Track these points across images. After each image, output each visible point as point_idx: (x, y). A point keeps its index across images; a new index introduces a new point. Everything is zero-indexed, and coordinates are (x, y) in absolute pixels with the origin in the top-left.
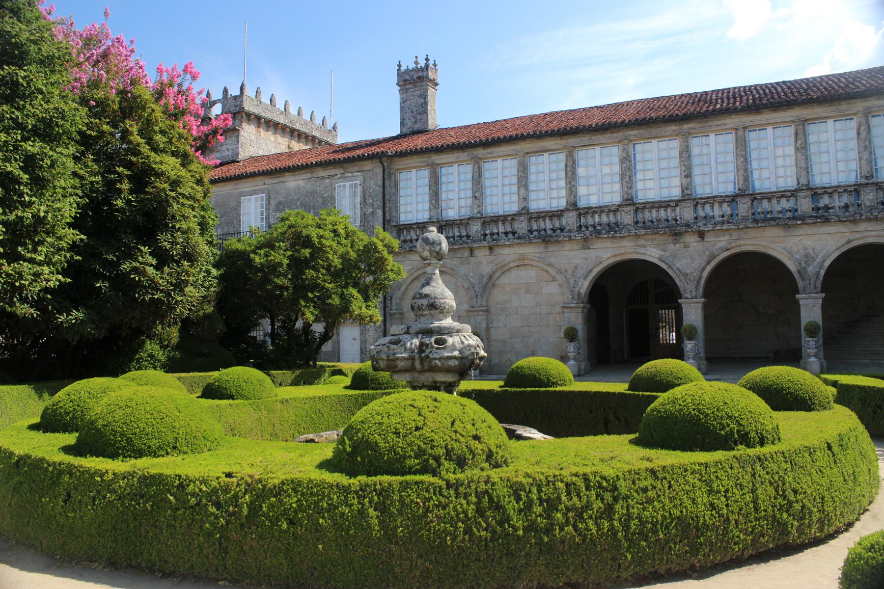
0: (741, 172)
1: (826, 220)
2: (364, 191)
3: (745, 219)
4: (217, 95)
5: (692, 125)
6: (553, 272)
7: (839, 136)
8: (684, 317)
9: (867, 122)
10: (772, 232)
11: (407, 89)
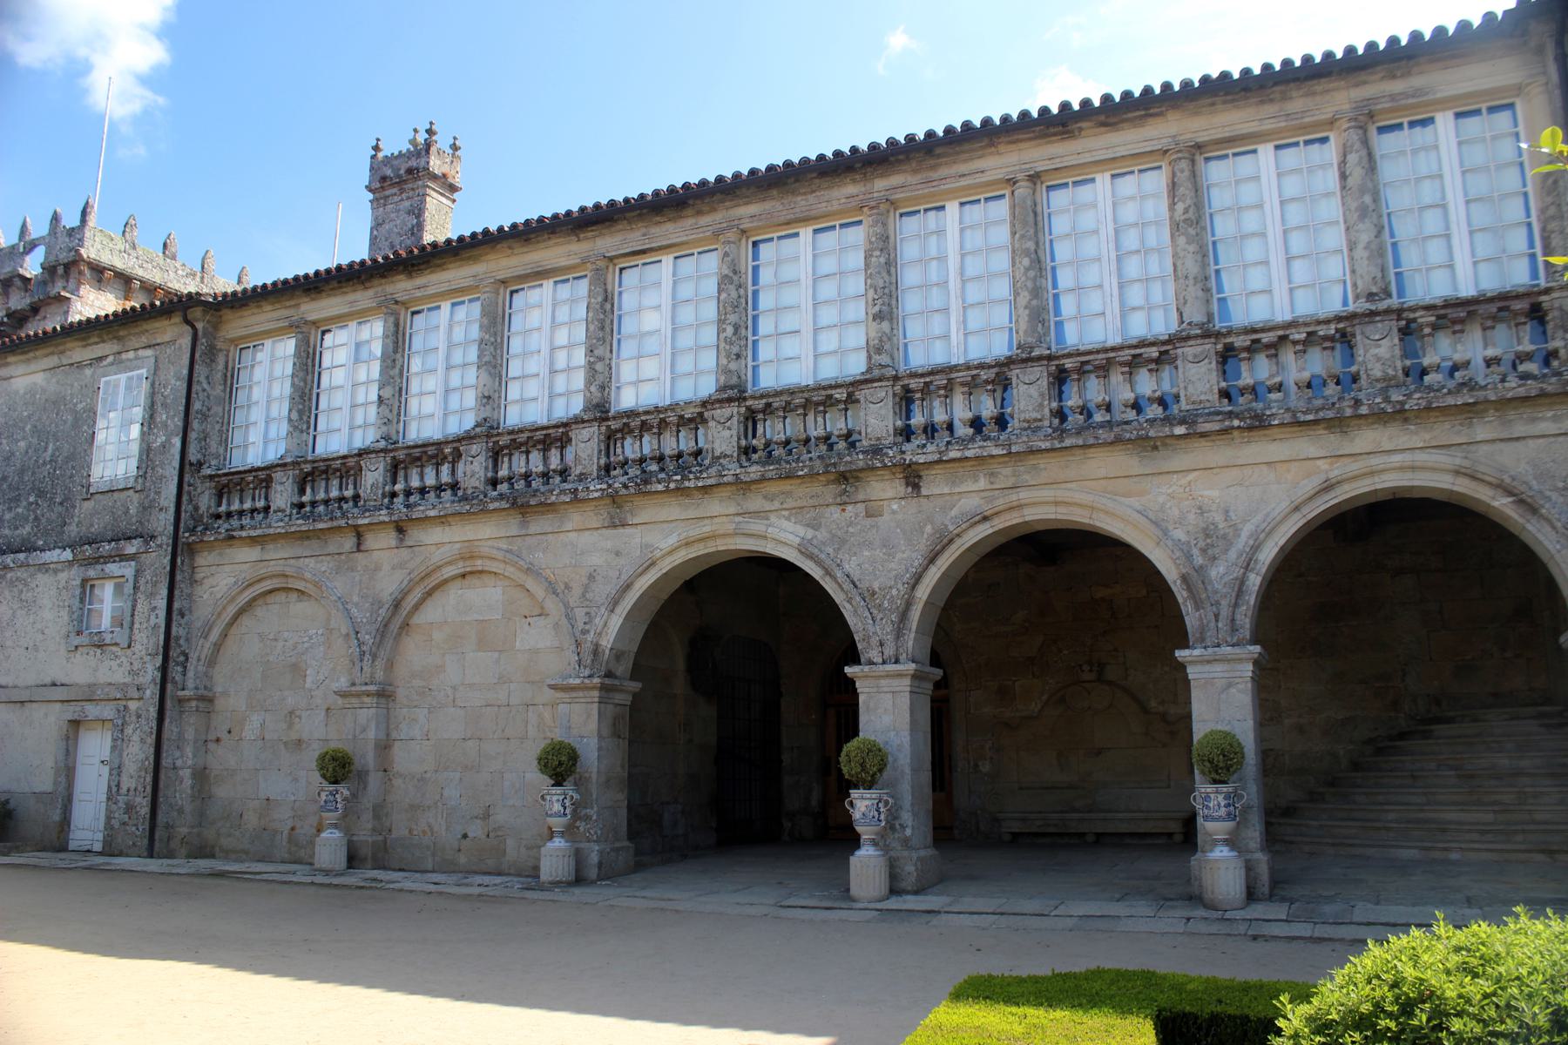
0: (1024, 297)
1: (1258, 424)
2: (152, 394)
3: (1032, 427)
4: (39, 229)
5: (896, 180)
6: (539, 591)
7: (1292, 186)
8: (863, 719)
9: (1365, 142)
10: (1106, 464)
11: (386, 197)
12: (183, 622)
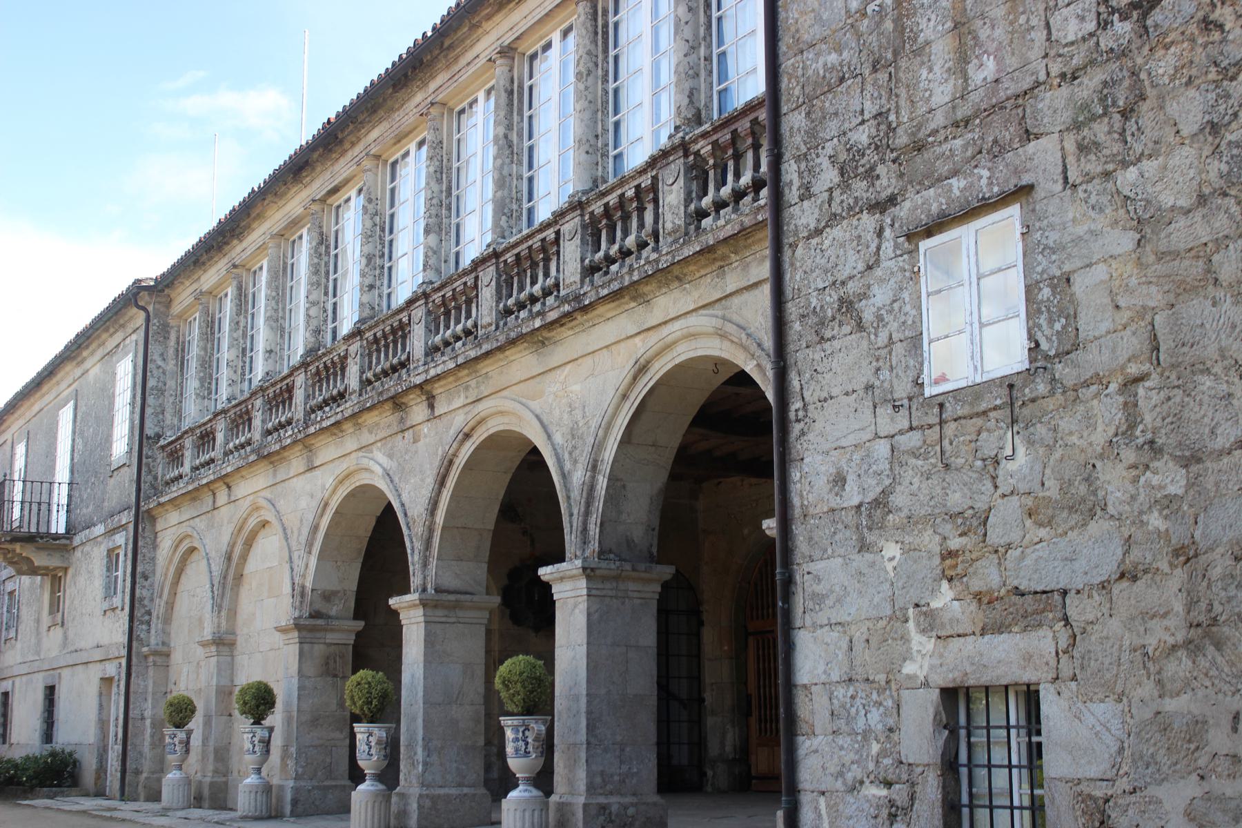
12: (146, 584)
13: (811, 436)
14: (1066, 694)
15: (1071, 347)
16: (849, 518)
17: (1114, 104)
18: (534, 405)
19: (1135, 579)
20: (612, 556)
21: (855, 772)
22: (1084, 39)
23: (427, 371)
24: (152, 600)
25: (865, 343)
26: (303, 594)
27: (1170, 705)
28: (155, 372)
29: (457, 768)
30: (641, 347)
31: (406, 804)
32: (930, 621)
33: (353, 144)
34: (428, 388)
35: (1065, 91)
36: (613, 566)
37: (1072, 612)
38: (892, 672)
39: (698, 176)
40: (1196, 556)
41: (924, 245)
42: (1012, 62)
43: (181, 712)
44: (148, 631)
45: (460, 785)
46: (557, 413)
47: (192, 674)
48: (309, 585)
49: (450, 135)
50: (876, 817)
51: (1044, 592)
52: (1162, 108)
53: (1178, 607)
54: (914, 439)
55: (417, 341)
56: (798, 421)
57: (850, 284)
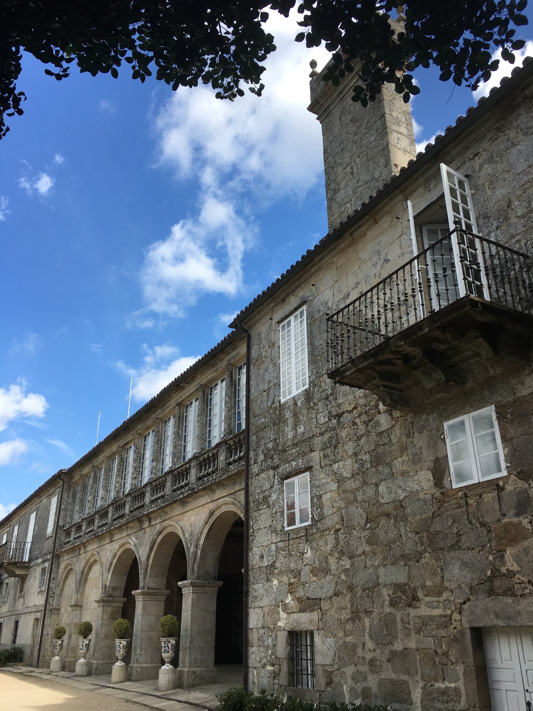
12: (54, 582)
13: (255, 541)
14: (321, 635)
15: (322, 518)
16: (264, 570)
17: (332, 444)
18: (181, 523)
19: (338, 596)
20: (201, 578)
21: (264, 661)
22: (325, 423)
23: (148, 510)
24: (55, 588)
25: (270, 512)
26: (105, 588)
27: (349, 639)
28: (64, 503)
29: (151, 656)
30: (212, 506)
31: (132, 670)
32: (286, 607)
33: (133, 429)
34: (149, 515)
35: (320, 438)
36: (201, 582)
37: (322, 606)
38: (275, 624)
39: (230, 451)
40: (353, 589)
41: (286, 482)
42: (308, 428)
43: (60, 633)
44: (53, 600)
45: (151, 663)
46: (187, 527)
47: (67, 618)
48: (108, 584)
49: (162, 429)
50: (270, 677)
51: (315, 599)
52: (343, 446)
53: (349, 606)
54: (281, 545)
55: (148, 498)
56: (252, 536)
57: (266, 492)
